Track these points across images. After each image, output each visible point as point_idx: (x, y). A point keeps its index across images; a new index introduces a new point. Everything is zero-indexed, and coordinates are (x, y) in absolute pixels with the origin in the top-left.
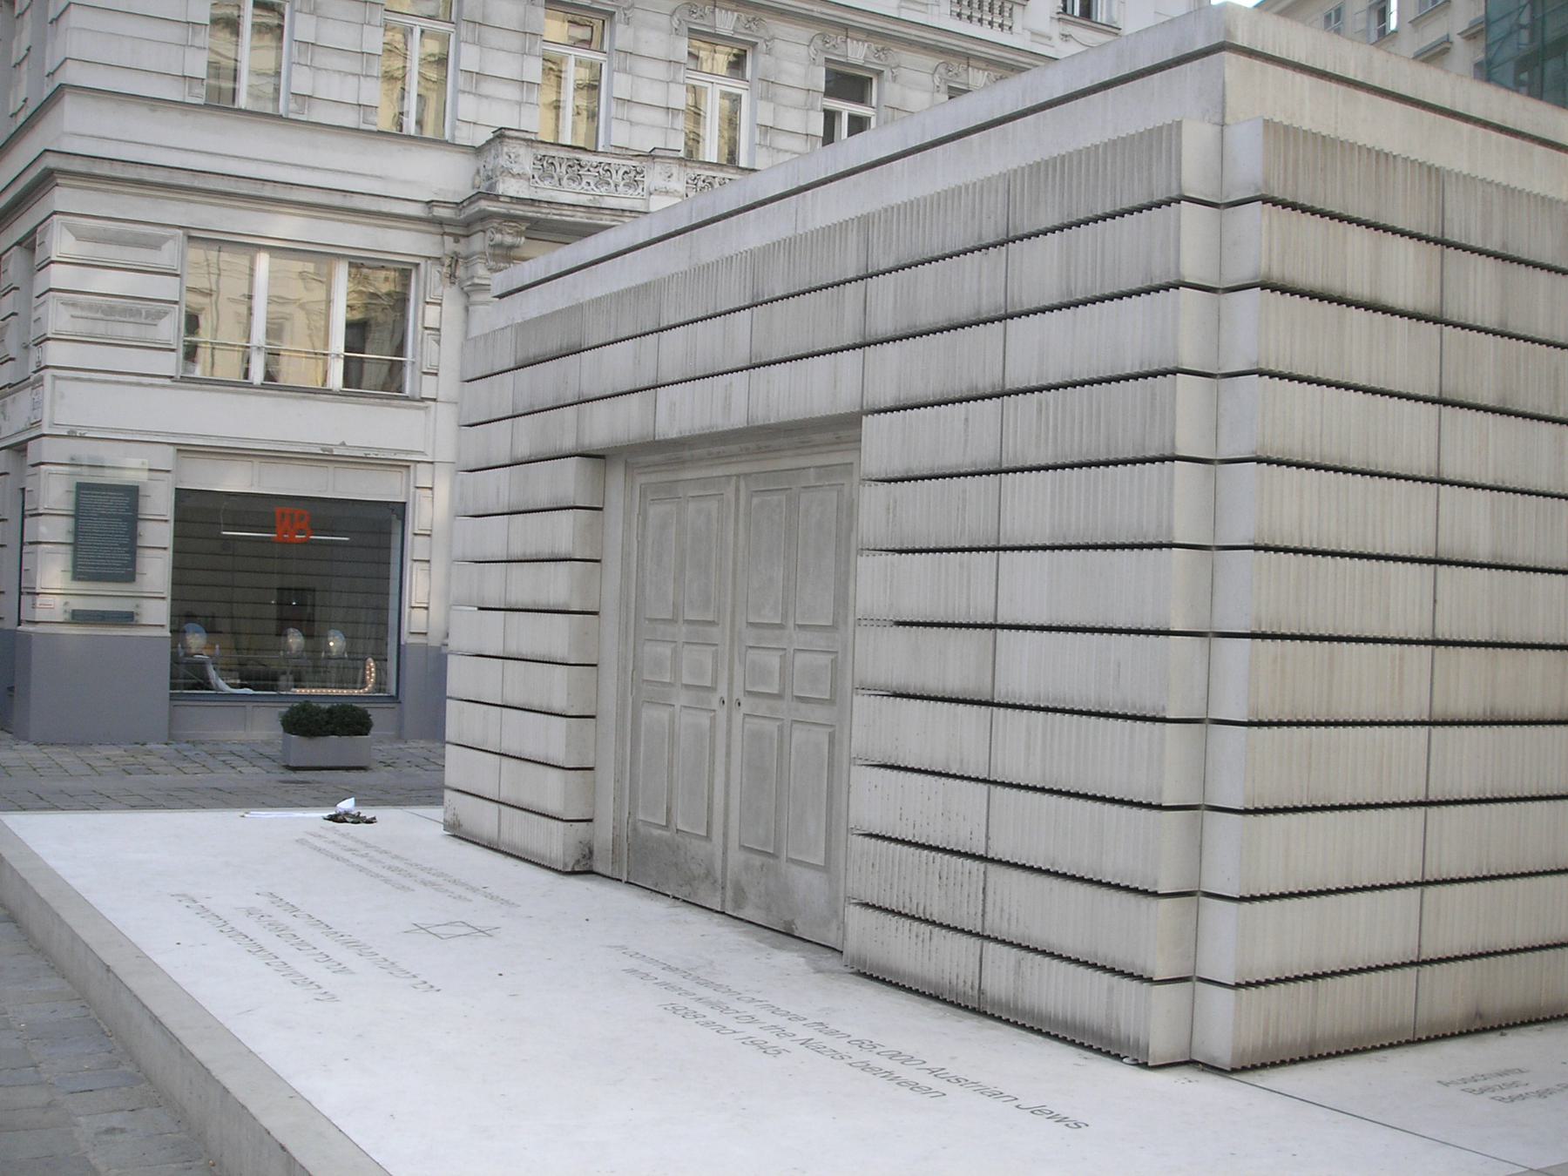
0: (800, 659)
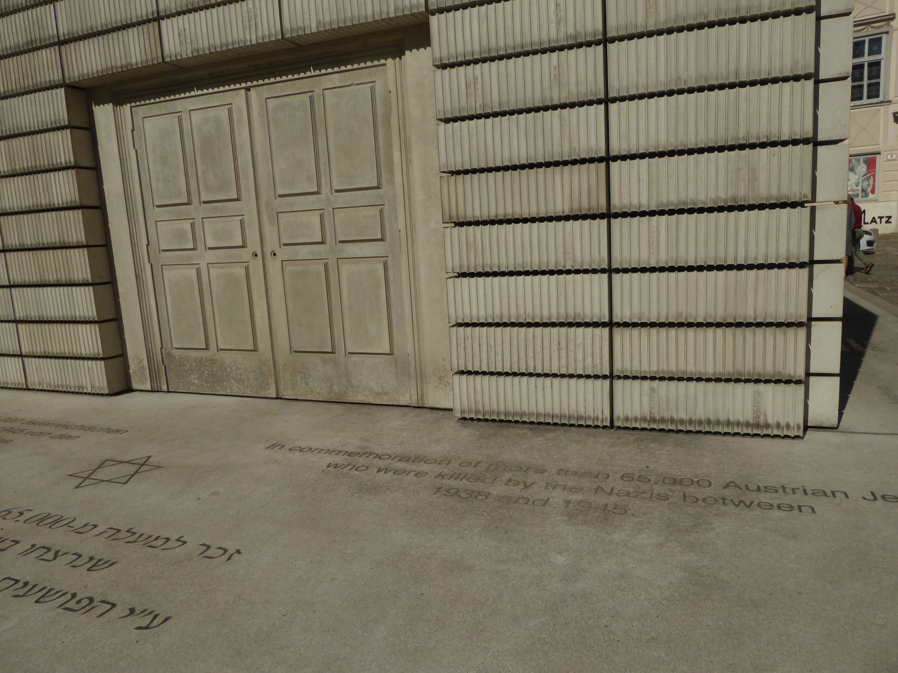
0: (340, 215)
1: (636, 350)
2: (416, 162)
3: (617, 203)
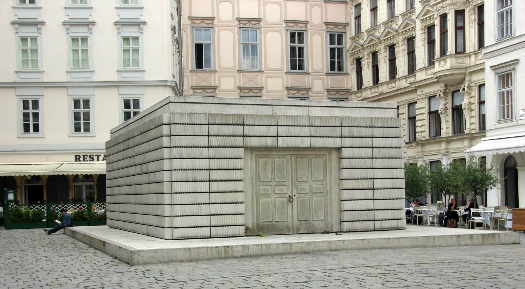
0: (314, 186)
1: (379, 215)
2: (333, 176)
3: (375, 187)
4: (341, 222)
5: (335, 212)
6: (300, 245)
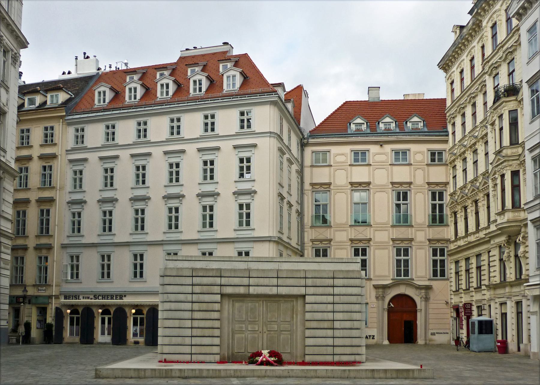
1: (338, 350)
3: (335, 327)
4: (305, 355)
5: (299, 346)
6: (228, 372)
